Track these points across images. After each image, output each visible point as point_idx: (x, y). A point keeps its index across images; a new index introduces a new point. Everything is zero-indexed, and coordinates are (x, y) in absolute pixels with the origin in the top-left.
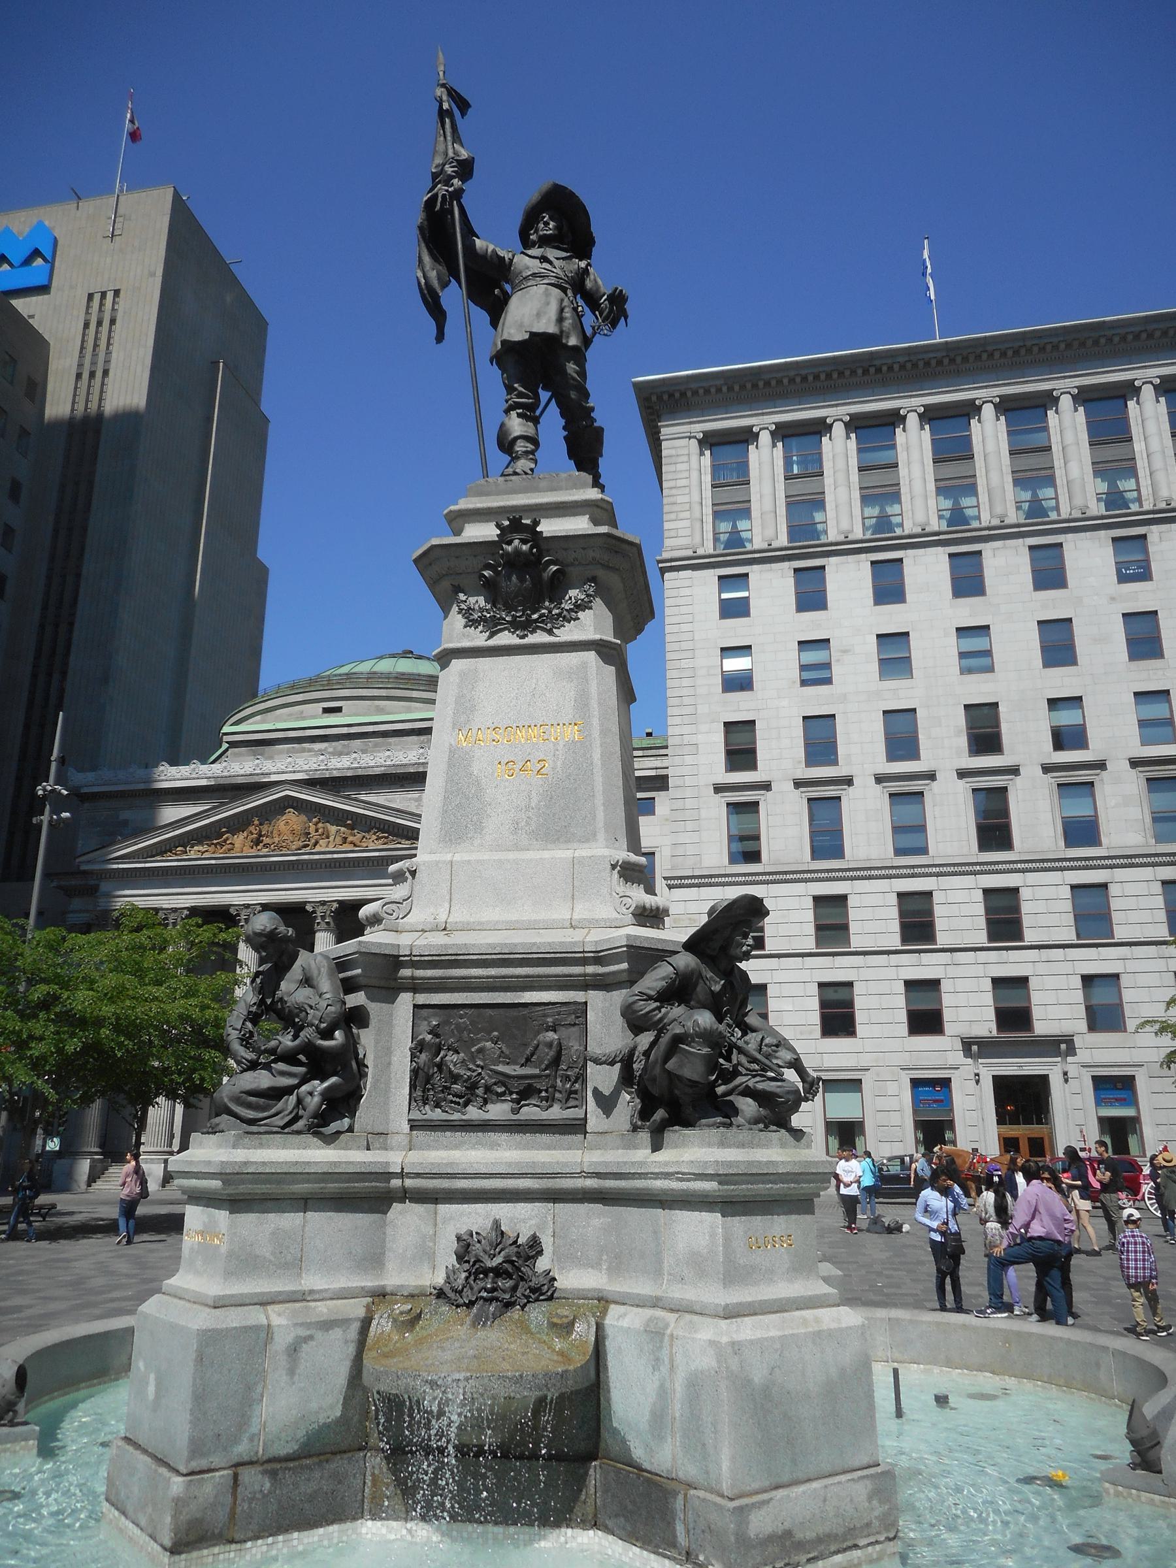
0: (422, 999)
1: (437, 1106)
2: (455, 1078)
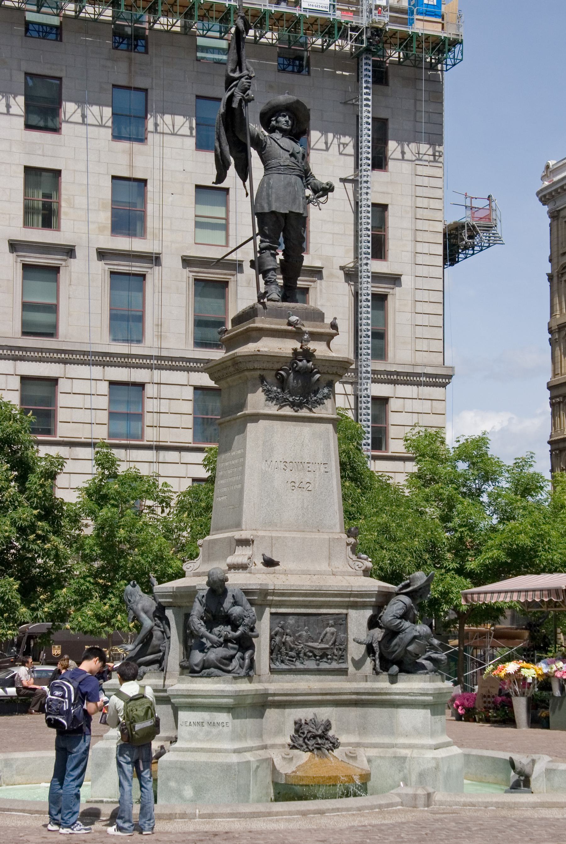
0: (274, 610)
1: (282, 662)
2: (292, 649)
